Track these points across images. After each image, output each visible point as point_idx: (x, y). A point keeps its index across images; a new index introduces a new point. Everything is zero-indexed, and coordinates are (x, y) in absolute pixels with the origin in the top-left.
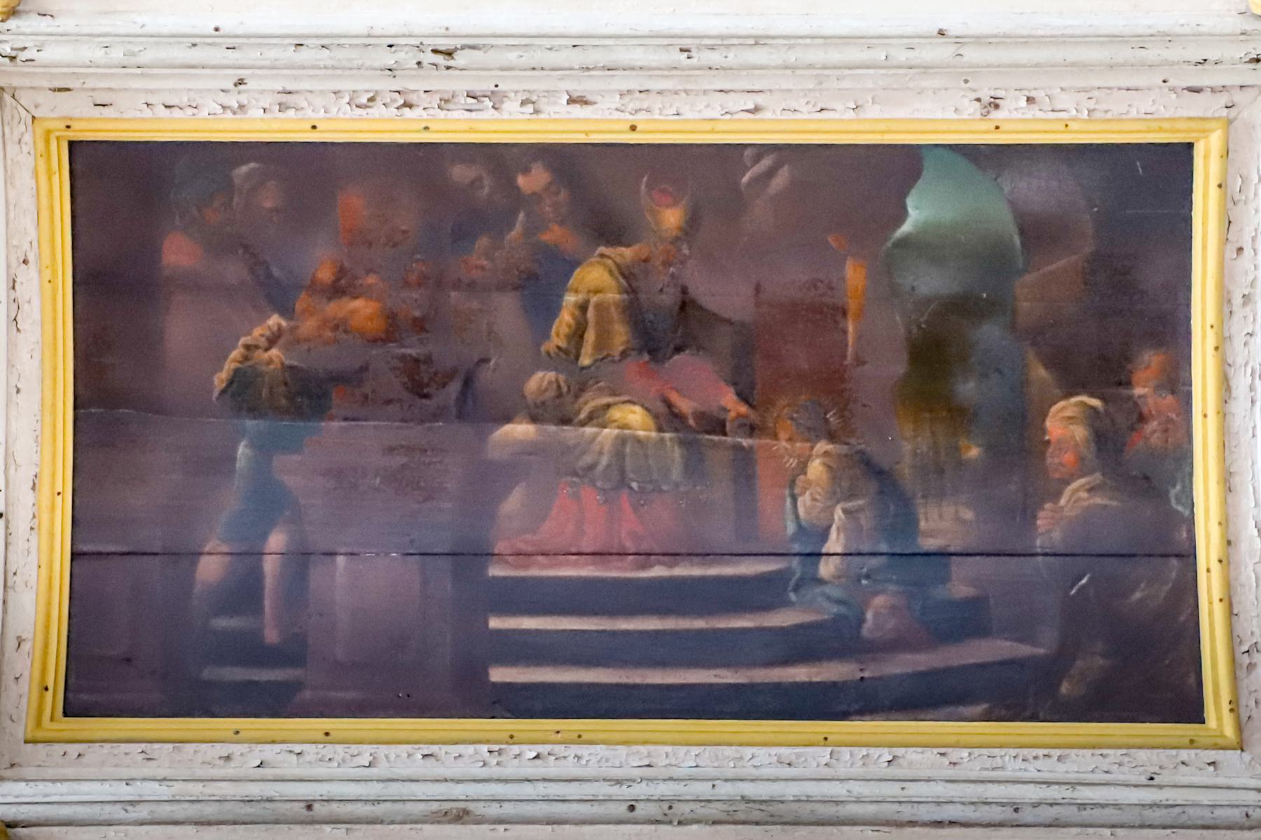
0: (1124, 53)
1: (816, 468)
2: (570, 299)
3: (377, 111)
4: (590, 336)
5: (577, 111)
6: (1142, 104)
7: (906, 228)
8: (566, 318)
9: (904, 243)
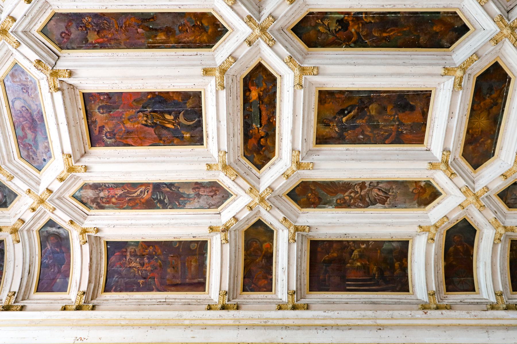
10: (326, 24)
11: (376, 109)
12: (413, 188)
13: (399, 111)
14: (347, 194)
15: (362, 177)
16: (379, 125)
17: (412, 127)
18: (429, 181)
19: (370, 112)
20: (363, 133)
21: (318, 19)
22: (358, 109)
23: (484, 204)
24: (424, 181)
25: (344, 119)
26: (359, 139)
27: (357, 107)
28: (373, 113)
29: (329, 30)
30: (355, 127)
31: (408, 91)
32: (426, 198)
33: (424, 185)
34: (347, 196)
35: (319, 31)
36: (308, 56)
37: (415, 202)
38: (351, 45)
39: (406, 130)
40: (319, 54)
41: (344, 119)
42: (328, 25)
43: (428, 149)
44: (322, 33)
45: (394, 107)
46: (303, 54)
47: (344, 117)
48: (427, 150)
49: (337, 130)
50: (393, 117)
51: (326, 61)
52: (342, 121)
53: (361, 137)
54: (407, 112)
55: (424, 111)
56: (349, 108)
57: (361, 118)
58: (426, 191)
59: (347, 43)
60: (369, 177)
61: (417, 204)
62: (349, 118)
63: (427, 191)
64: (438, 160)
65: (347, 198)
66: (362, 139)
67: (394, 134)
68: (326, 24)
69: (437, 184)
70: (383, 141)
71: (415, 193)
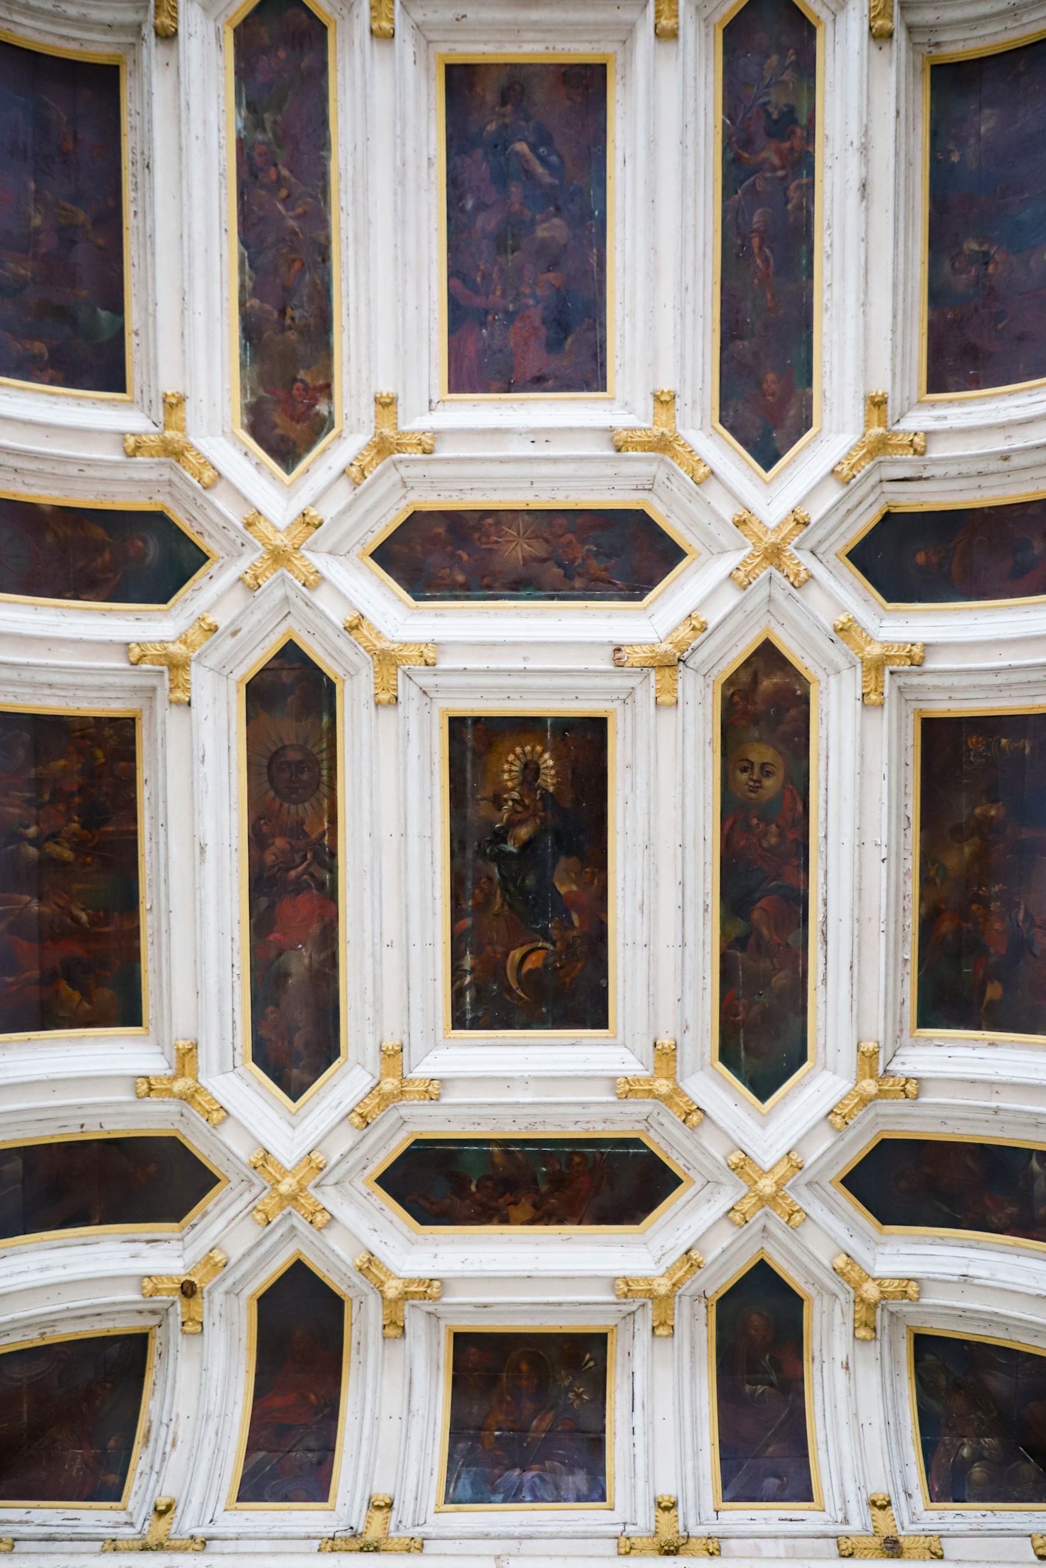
0: (152, 364)
1: (22, 272)
2: (74, 208)
3: (131, 155)
4: (63, 212)
5: (132, 214)
6: (137, 377)
7: (99, 310)
8: (69, 206)
9: (95, 311)
10: (784, 77)
11: (553, 238)
12: (308, 379)
13: (546, 308)
14: (285, 172)
15: (343, 216)
16: (506, 251)
17: (500, 351)
18: (332, 426)
19: (543, 221)
20: (480, 207)
21: (797, 53)
22: (551, 186)
23: (264, 586)
24: (330, 413)
25: (522, 147)
26: (461, 198)
27: (557, 182)
28: (542, 232)
29: (767, 86)
30: (501, 179)
31: (603, 326)
32: (275, 426)
33: (318, 414)
34: (279, 173)
35: (768, 56)
36: (702, 24)
37: (262, 392)
38: (729, 150)
39: (492, 334)
40: (707, 59)
41: (522, 147)
42: (782, 82)
43: (433, 404)
44: (761, 65)
45: (558, 290)
46: (709, 10)
47: (529, 145)
48: (430, 402)
49: (489, 128)
50: (527, 291)
51: (690, 67)
52: (520, 140)
53: (469, 204)
54: (543, 331)
55: (548, 380)
56: (554, 159)
57: (526, 197)
58: (298, 422)
59: (734, 139)
60: (343, 236)
61: (254, 400)
62: (527, 161)
63: (299, 427)
64: (405, 424)
65: (273, 174)
66: (464, 206)
67: (479, 301)
68: (784, 77)
69: (324, 451)
70: (456, 272)
71: (291, 389)
